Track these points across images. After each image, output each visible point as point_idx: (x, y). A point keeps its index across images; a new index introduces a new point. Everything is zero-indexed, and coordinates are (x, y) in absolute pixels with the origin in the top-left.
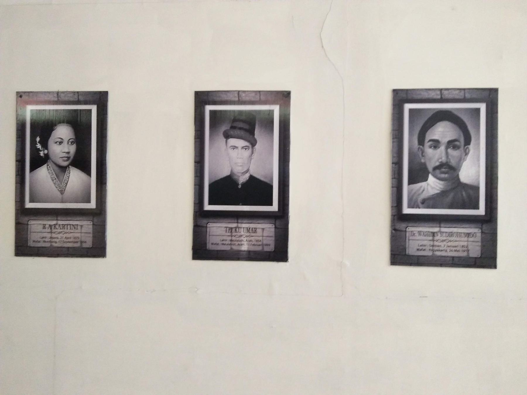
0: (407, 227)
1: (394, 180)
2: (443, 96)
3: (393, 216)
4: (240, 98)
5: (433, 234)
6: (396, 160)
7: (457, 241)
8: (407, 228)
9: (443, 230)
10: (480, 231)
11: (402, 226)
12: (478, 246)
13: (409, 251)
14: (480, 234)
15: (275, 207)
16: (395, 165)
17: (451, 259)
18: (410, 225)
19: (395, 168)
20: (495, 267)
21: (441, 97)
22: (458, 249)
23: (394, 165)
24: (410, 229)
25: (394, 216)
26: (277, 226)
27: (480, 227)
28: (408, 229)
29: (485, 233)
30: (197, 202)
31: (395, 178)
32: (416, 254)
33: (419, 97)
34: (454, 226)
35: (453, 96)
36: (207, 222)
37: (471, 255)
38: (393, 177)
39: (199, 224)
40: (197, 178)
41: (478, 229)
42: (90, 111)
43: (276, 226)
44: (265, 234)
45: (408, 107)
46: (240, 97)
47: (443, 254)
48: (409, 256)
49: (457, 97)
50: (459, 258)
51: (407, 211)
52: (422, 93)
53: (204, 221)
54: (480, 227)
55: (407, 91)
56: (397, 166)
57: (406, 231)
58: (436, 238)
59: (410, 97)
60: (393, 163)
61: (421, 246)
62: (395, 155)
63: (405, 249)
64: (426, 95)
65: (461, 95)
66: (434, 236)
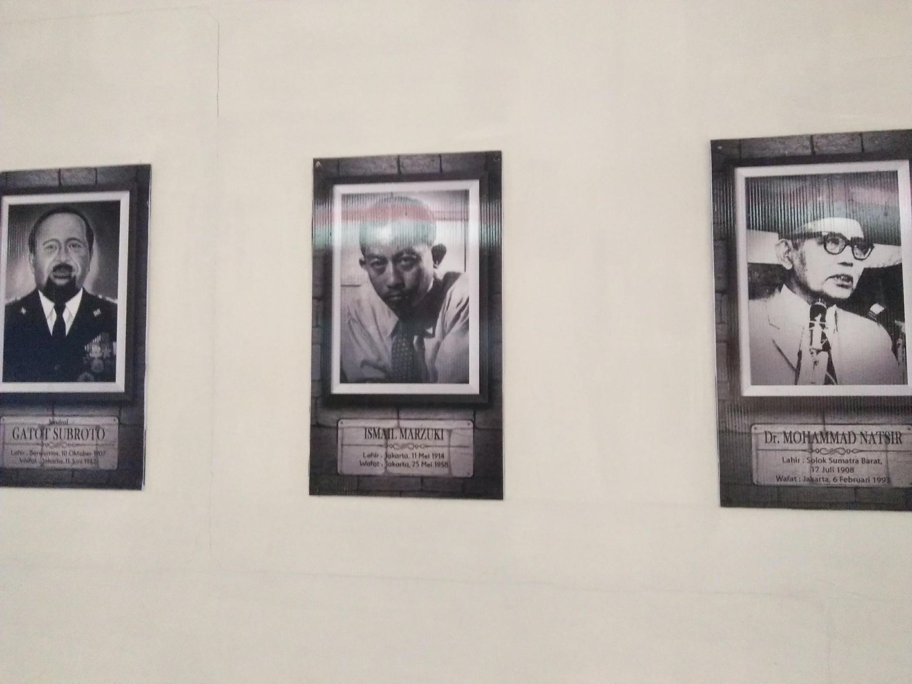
0: (755, 424)
1: (316, 329)
2: (816, 149)
4: (402, 169)
5: (387, 433)
6: (319, 292)
7: (802, 450)
9: (404, 424)
10: (471, 425)
11: (330, 417)
12: (467, 454)
13: (342, 467)
15: (119, 385)
17: (419, 480)
18: (345, 416)
22: (429, 461)
24: (344, 424)
26: (122, 421)
29: (479, 429)
30: (318, 377)
32: (356, 473)
33: (360, 172)
34: (424, 416)
41: (113, 418)
42: (117, 204)
43: (477, 425)
44: (455, 440)
46: (403, 167)
50: (434, 479)
56: (321, 303)
58: (815, 446)
61: (369, 456)
62: (318, 283)
63: (335, 463)
66: (810, 443)
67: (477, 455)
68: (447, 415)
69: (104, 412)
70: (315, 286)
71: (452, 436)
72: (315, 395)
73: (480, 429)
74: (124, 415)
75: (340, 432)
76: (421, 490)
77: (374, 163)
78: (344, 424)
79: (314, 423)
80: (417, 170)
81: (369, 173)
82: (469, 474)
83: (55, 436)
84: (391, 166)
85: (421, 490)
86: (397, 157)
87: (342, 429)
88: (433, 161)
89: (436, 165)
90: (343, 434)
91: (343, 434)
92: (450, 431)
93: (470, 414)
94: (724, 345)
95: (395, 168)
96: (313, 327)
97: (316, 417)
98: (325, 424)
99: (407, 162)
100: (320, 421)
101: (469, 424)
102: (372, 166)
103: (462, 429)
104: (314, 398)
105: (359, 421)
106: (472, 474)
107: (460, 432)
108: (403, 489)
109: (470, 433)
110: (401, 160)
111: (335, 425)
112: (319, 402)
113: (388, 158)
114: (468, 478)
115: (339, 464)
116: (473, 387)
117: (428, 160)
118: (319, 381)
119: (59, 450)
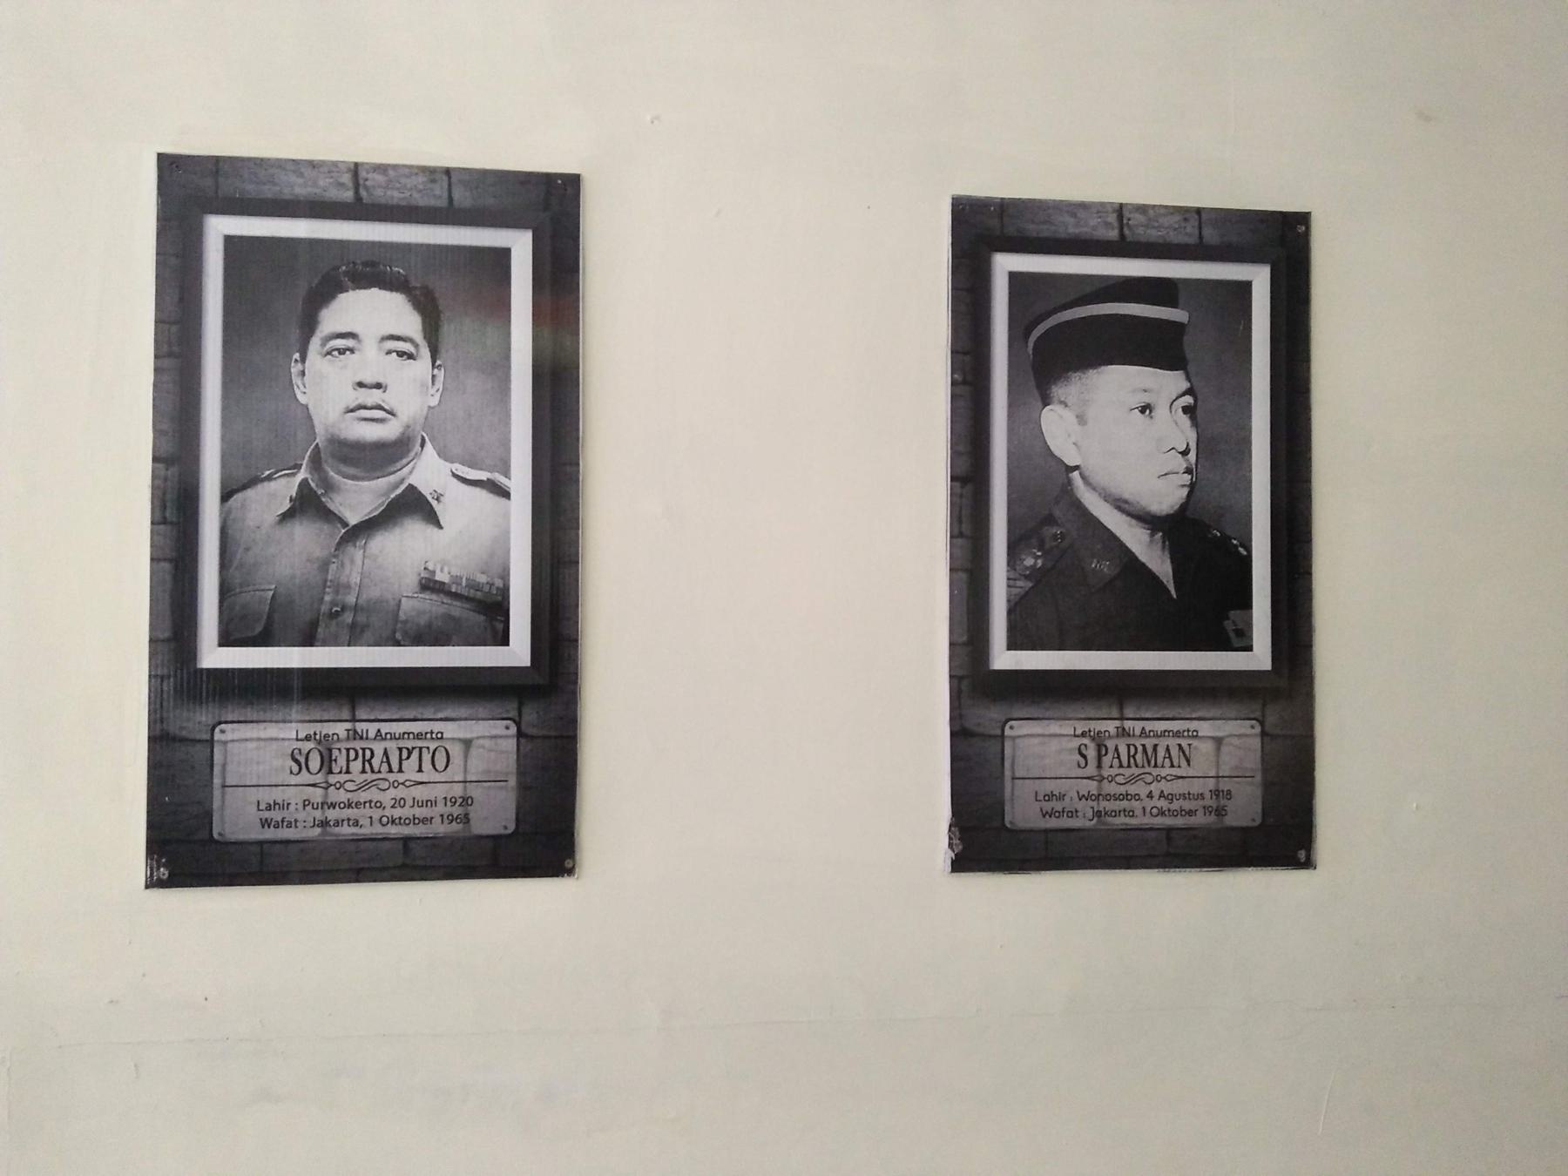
1: (959, 541)
3: (956, 681)
16: (962, 487)
19: (961, 496)
20: (960, 864)
21: (1122, 235)
23: (957, 484)
25: (961, 678)
28: (1011, 728)
31: (961, 535)
33: (1045, 231)
36: (211, 722)
37: (1230, 821)
38: (956, 532)
44: (478, 764)
45: (1005, 264)
47: (1134, 822)
49: (1175, 238)
51: (214, 656)
54: (1258, 714)
55: (1004, 207)
56: (969, 488)
57: (1003, 735)
59: (1011, 230)
60: (953, 479)
62: (961, 448)
63: (999, 808)
64: (1070, 227)
69: (481, 711)
70: (955, 454)
72: (960, 673)
73: (531, 738)
74: (530, 715)
75: (1008, 745)
77: (1074, 215)
79: (957, 728)
83: (295, 768)
84: (1107, 225)
87: (1014, 738)
88: (1186, 220)
89: (1192, 228)
90: (1014, 749)
91: (1014, 749)
93: (511, 708)
94: (964, 576)
95: (1113, 229)
98: (981, 730)
99: (1138, 218)
100: (970, 724)
101: (1253, 727)
102: (1071, 220)
103: (1240, 736)
104: (156, 678)
109: (1256, 743)
111: (998, 732)
112: (965, 685)
113: (1100, 208)
115: (1007, 808)
116: (518, 651)
117: (1177, 218)
119: (1139, 789)
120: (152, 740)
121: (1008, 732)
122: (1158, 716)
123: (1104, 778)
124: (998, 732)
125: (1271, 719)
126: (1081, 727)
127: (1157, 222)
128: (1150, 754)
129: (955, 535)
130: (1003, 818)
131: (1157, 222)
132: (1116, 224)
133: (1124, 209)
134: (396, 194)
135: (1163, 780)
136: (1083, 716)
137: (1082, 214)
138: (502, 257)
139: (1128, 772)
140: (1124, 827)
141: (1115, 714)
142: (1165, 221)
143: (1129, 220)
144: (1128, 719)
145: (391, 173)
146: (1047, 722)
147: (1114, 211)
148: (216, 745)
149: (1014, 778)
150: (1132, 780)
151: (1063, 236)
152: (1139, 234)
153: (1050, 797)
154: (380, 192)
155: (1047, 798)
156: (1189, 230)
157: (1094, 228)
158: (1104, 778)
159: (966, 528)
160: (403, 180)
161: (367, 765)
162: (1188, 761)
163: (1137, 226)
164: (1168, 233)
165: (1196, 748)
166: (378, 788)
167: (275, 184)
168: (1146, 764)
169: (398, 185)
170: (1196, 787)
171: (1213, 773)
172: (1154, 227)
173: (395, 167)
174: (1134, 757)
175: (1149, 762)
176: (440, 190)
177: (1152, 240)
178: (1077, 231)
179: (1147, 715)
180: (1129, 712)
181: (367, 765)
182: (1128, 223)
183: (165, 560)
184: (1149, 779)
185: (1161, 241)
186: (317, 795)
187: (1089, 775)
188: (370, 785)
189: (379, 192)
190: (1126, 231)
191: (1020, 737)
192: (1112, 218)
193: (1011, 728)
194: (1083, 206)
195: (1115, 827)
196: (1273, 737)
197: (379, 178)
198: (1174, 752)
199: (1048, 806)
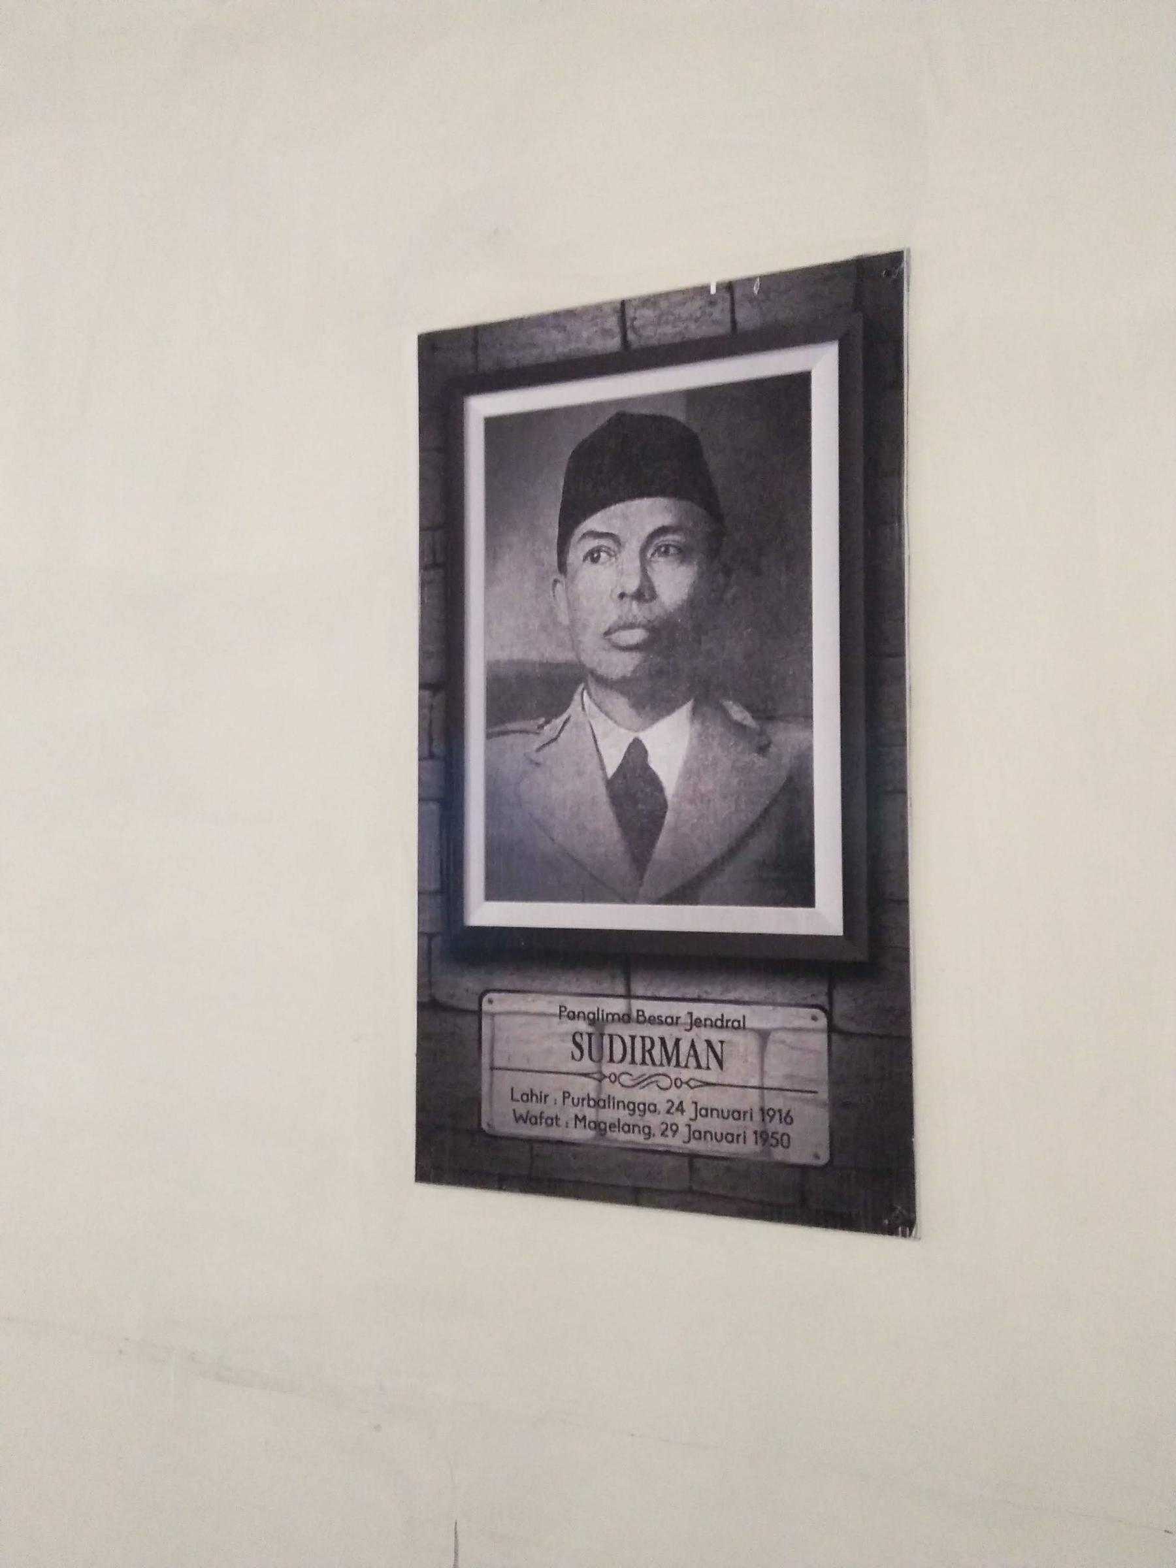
8: (485, 1000)
10: (823, 1022)
14: (824, 1036)
18: (497, 984)
24: (496, 1003)
27: (822, 1000)
28: (490, 1002)
29: (840, 1032)
35: (681, 326)
36: (479, 988)
39: (442, 995)
40: (429, 764)
48: (494, 1139)
49: (696, 331)
52: (541, 336)
53: (467, 983)
64: (558, 346)
65: (716, 324)
67: (839, 1105)
68: (756, 993)
71: (771, 1048)
72: (427, 929)
76: (690, 1190)
77: (563, 329)
78: (496, 1003)
79: (426, 1000)
80: (667, 333)
81: (549, 355)
82: (817, 1157)
84: (606, 333)
85: (690, 1190)
86: (619, 306)
87: (493, 1015)
90: (493, 1029)
91: (493, 1029)
92: (764, 1036)
95: (613, 337)
96: (421, 759)
97: (430, 984)
102: (556, 335)
105: (530, 997)
106: (824, 1158)
107: (790, 1038)
108: (641, 1184)
110: (630, 313)
114: (815, 1168)
118: (436, 893)
120: (421, 1006)
121: (486, 1007)
122: (677, 995)
123: (605, 1077)
124: (475, 1007)
125: (840, 1008)
126: (574, 1004)
127: (673, 315)
128: (670, 1049)
129: (426, 756)
130: (480, 1120)
131: (673, 315)
132: (617, 330)
133: (627, 306)
134: (669, 329)
135: (685, 1086)
136: (579, 991)
137: (570, 324)
138: (493, 425)
139: (637, 1070)
140: (629, 1146)
141: (620, 989)
142: (684, 312)
143: (635, 318)
144: (637, 997)
145: (663, 304)
146: (533, 995)
147: (615, 311)
148: (483, 1015)
149: (492, 1068)
150: (641, 1082)
151: (552, 359)
152: (649, 337)
153: (529, 1096)
154: (652, 333)
155: (525, 1098)
156: (717, 315)
157: (589, 341)
158: (605, 1077)
159: (438, 749)
160: (677, 312)
161: (647, 1055)
162: (720, 1063)
163: (644, 326)
164: (686, 328)
165: (730, 1042)
166: (658, 1086)
167: (534, 346)
168: (665, 1061)
169: (671, 318)
170: (724, 1100)
171: (755, 1082)
172: (667, 323)
173: (667, 295)
174: (650, 1052)
175: (669, 1060)
176: (720, 313)
177: (667, 340)
178: (566, 350)
179: (663, 993)
180: (638, 988)
181: (647, 1055)
182: (633, 327)
183: (432, 800)
184: (665, 1082)
185: (678, 340)
186: (589, 1087)
187: (585, 1072)
188: (649, 1081)
189: (649, 331)
190: (631, 336)
191: (500, 1014)
192: (612, 323)
193: (490, 1002)
194: (571, 314)
195: (617, 1145)
196: (847, 1035)
197: (649, 313)
198: (701, 1047)
199: (521, 1109)
